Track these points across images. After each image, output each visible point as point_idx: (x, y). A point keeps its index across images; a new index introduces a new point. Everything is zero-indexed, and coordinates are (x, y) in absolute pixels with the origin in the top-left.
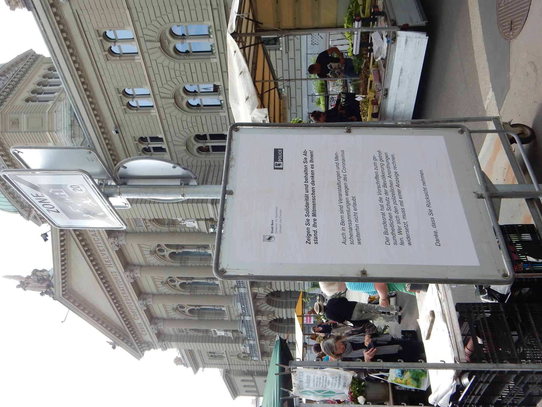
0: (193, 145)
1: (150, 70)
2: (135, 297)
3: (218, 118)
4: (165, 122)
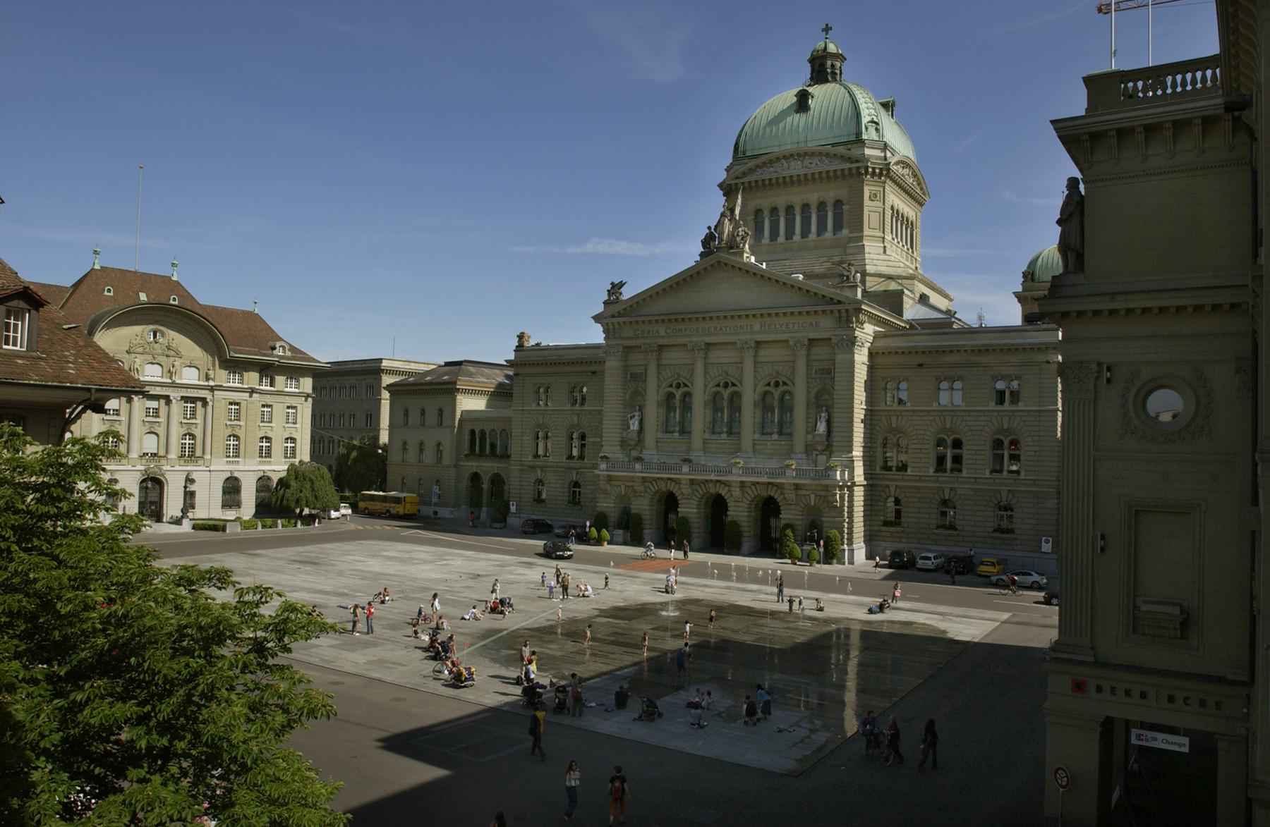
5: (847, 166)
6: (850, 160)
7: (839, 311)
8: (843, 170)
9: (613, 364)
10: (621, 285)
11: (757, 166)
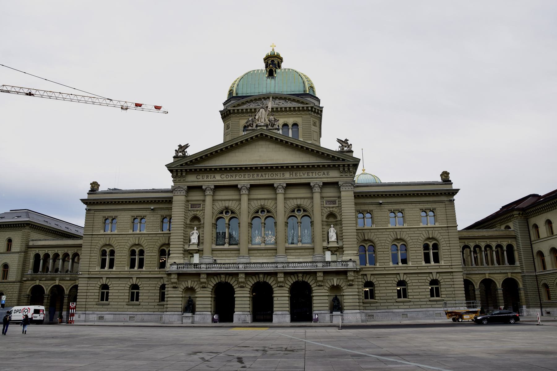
0: (367, 244)
1: (416, 230)
2: (253, 182)
3: (388, 261)
4: (384, 230)
5: (302, 105)
6: (302, 103)
7: (344, 165)
8: (299, 108)
9: (179, 200)
10: (187, 146)
11: (247, 102)
